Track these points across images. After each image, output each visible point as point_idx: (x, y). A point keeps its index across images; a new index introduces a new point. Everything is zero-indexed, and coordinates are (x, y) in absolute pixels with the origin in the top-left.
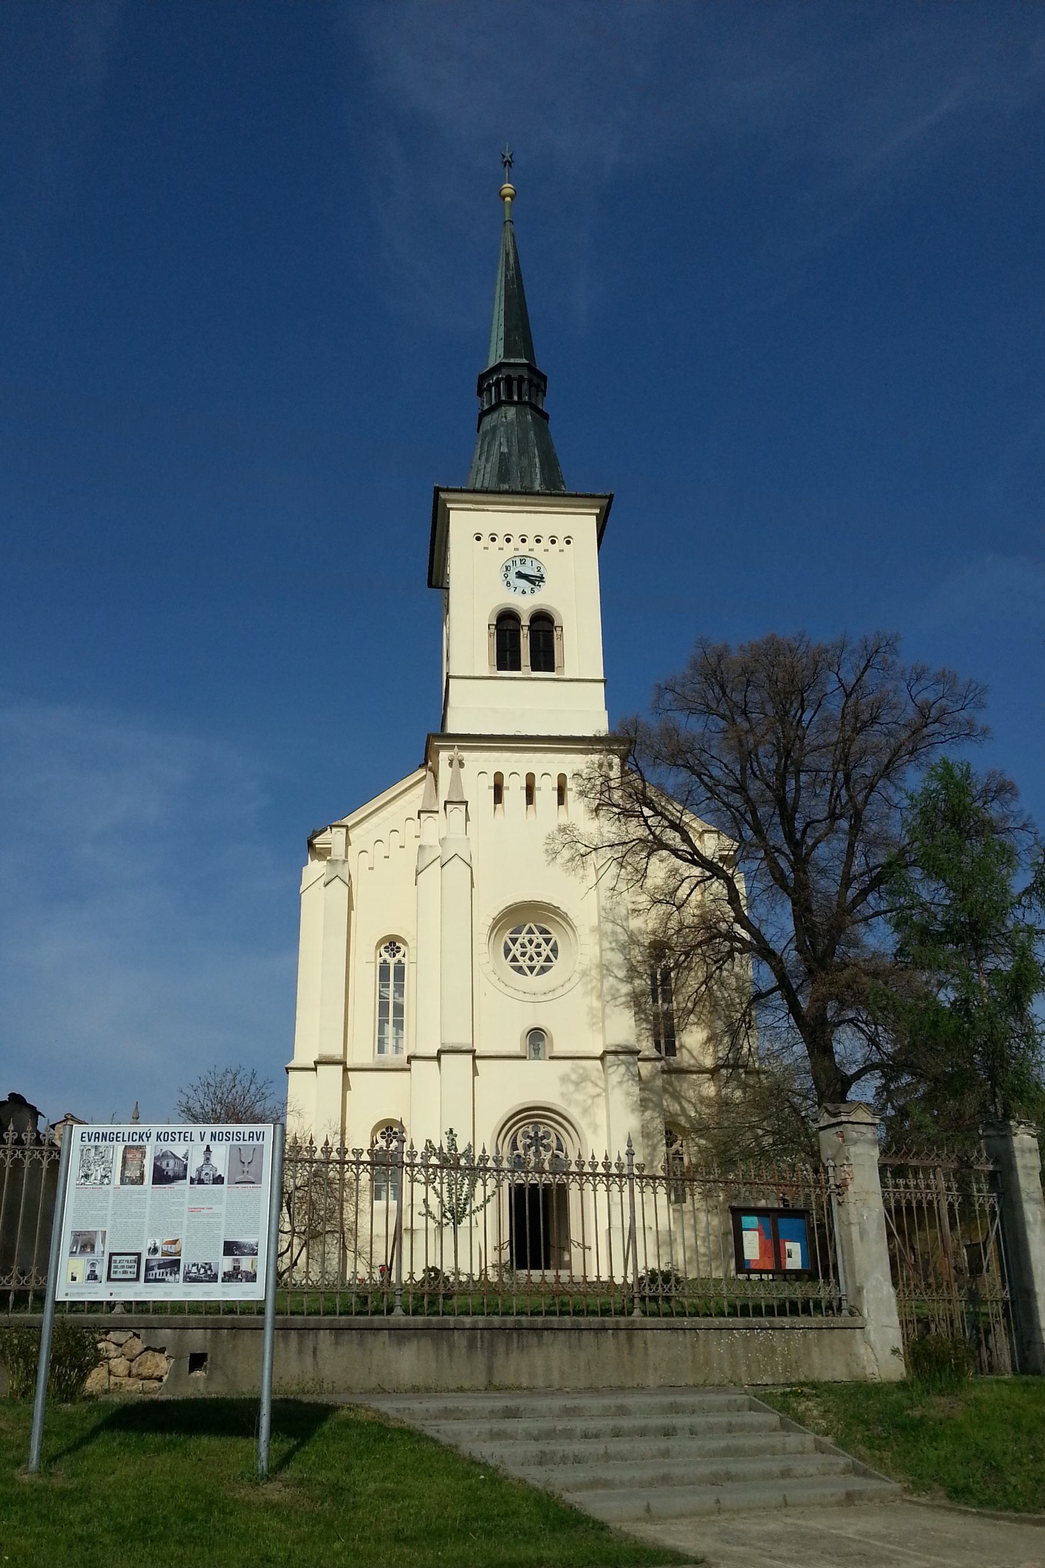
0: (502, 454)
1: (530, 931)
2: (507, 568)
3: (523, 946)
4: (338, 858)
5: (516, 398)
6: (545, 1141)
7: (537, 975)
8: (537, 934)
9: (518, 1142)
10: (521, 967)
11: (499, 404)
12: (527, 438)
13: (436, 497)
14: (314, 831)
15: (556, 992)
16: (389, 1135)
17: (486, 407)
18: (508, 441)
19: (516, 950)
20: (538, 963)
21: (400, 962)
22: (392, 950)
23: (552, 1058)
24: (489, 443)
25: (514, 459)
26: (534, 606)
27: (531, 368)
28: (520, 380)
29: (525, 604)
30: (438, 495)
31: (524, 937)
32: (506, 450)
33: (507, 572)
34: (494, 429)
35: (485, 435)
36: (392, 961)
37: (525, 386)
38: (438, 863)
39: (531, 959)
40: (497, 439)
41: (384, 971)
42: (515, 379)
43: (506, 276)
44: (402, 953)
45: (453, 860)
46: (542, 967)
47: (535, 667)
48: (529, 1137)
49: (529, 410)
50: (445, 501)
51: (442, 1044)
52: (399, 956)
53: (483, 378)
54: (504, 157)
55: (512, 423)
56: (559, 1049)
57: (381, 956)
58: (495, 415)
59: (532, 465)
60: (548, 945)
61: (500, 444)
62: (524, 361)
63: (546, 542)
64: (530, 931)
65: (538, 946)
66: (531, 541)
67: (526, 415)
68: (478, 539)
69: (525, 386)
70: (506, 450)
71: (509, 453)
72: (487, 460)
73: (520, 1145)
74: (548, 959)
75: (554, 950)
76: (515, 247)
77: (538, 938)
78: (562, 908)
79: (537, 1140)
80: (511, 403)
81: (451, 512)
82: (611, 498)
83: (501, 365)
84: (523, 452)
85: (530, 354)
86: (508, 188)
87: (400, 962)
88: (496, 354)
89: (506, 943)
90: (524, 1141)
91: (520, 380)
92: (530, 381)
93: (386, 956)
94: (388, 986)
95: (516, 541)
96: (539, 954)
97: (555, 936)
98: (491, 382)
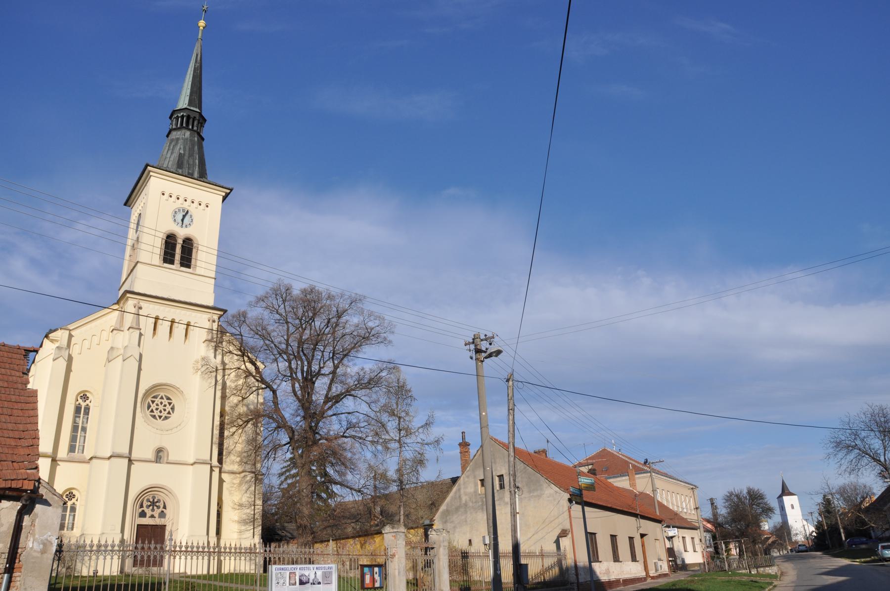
0: (180, 154)
2: (175, 212)
4: (63, 346)
5: (190, 127)
6: (157, 504)
7: (163, 420)
9: (144, 503)
10: (155, 416)
11: (182, 127)
12: (194, 149)
14: (51, 330)
15: (173, 430)
16: (70, 496)
17: (174, 127)
18: (184, 148)
19: (153, 407)
21: (88, 405)
22: (84, 398)
23: (167, 463)
24: (174, 146)
25: (186, 157)
26: (186, 234)
27: (200, 114)
29: (182, 233)
31: (158, 401)
32: (182, 152)
34: (178, 139)
35: (172, 140)
36: (83, 404)
37: (196, 123)
38: (120, 358)
40: (179, 145)
41: (78, 409)
43: (195, 65)
44: (89, 400)
45: (130, 358)
46: (166, 417)
47: (182, 265)
48: (149, 501)
49: (196, 135)
50: (150, 171)
51: (113, 452)
52: (88, 402)
53: (174, 112)
54: (203, 7)
55: (187, 139)
56: (172, 458)
57: (78, 401)
58: (179, 133)
59: (194, 165)
60: (170, 405)
61: (180, 148)
62: (198, 110)
63: (196, 204)
65: (165, 406)
66: (189, 201)
67: (195, 137)
68: (163, 194)
69: (196, 123)
70: (182, 152)
71: (184, 154)
72: (172, 153)
73: (144, 505)
74: (169, 413)
75: (173, 409)
76: (201, 53)
77: (165, 402)
79: (154, 503)
80: (189, 129)
82: (231, 190)
83: (186, 109)
84: (191, 155)
85: (200, 108)
86: (202, 23)
87: (88, 405)
88: (183, 102)
89: (149, 403)
90: (147, 503)
92: (199, 120)
93: (80, 401)
94: (79, 417)
95: (181, 200)
97: (174, 401)
98: (179, 115)
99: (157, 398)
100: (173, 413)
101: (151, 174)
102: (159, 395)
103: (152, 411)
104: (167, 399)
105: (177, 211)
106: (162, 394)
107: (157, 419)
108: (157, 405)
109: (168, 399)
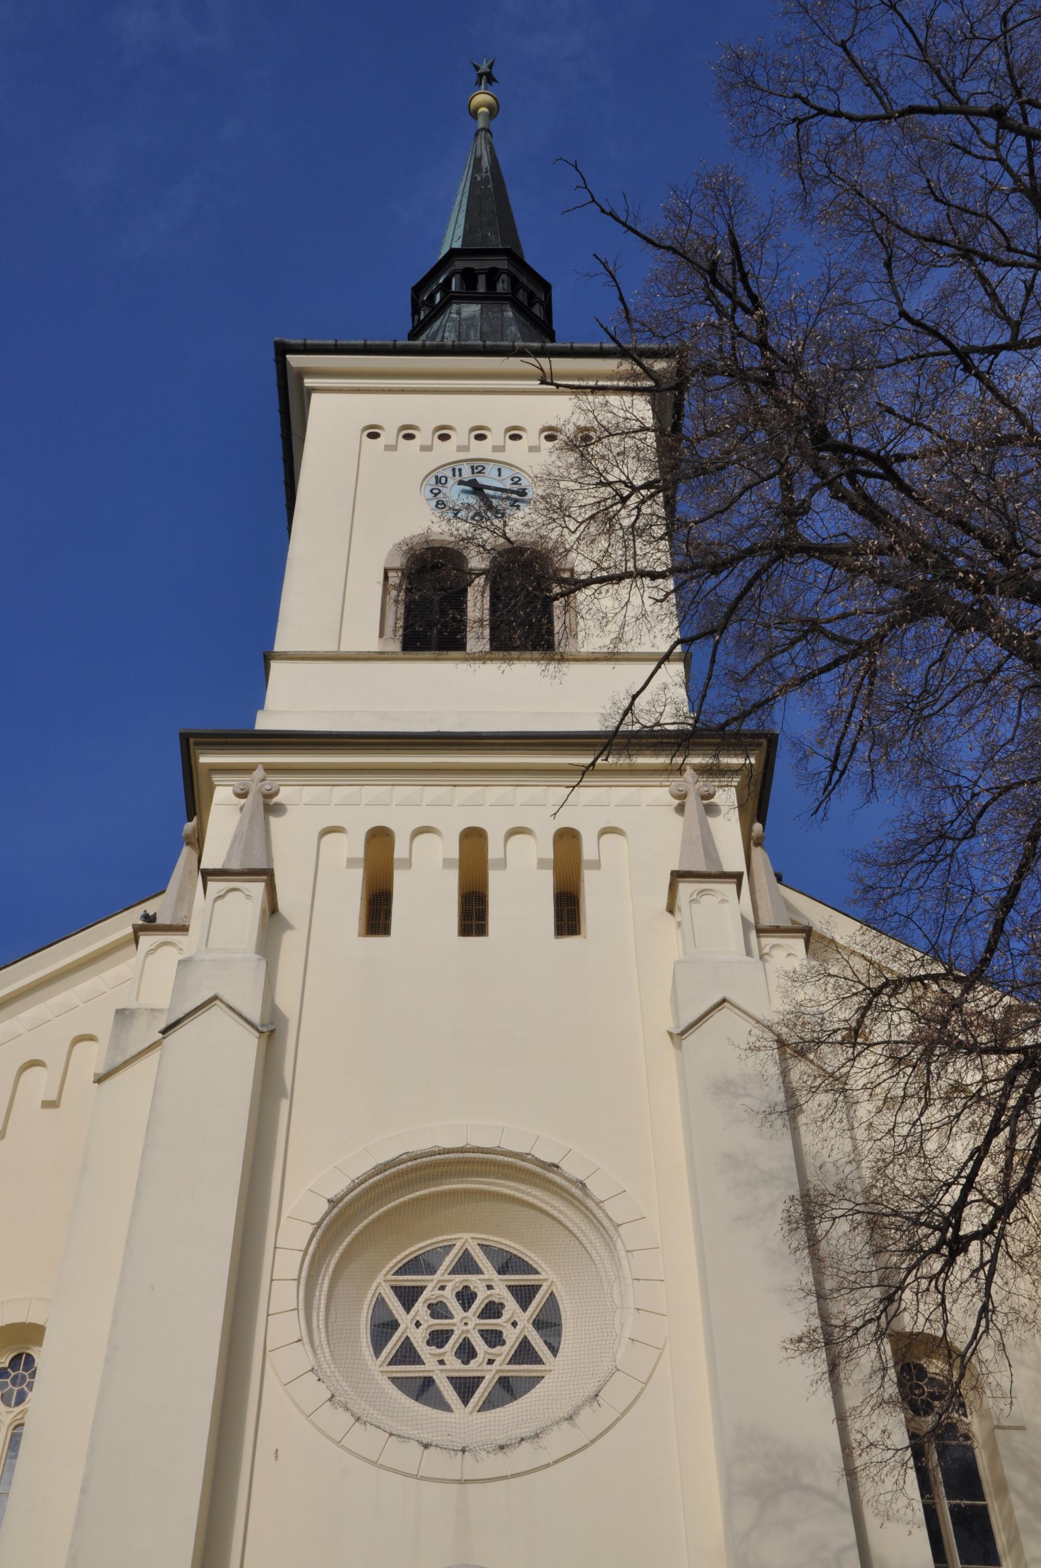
1: (466, 1265)
2: (438, 480)
10: (428, 1382)
13: (282, 366)
15: (546, 1440)
27: (515, 257)
28: (493, 275)
30: (285, 360)
33: (439, 487)
39: (467, 1352)
42: (481, 272)
43: (473, 178)
60: (524, 1307)
64: (466, 1265)
68: (374, 436)
74: (525, 1353)
78: (566, 1167)
81: (315, 397)
89: (380, 1303)
91: (493, 275)
96: (494, 1338)
99: (432, 1270)
100: (554, 1350)
101: (308, 382)
102: (448, 1248)
103: (407, 1354)
104: (502, 1270)
105: (449, 474)
106: (467, 1240)
107: (443, 1405)
108: (438, 1310)
109: (508, 1263)
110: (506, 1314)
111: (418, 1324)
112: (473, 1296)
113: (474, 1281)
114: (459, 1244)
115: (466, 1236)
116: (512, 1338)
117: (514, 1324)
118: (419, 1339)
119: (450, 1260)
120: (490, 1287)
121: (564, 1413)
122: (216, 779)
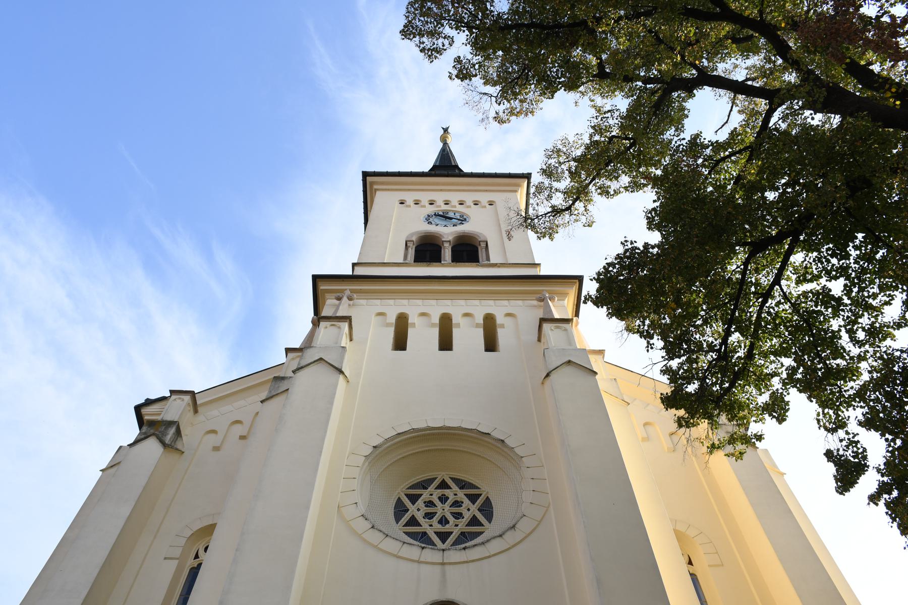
3: (429, 504)
8: (455, 488)
10: (425, 534)
20: (456, 528)
39: (443, 521)
46: (463, 534)
50: (372, 183)
74: (474, 521)
96: (458, 516)
97: (487, 489)
104: (461, 488)
109: (463, 484)
110: (464, 505)
111: (418, 510)
112: (447, 498)
113: (447, 492)
114: (439, 477)
115: (443, 473)
116: (467, 516)
117: (469, 510)
118: (419, 516)
119: (436, 483)
120: (456, 495)
121: (498, 534)
122: (327, 295)
